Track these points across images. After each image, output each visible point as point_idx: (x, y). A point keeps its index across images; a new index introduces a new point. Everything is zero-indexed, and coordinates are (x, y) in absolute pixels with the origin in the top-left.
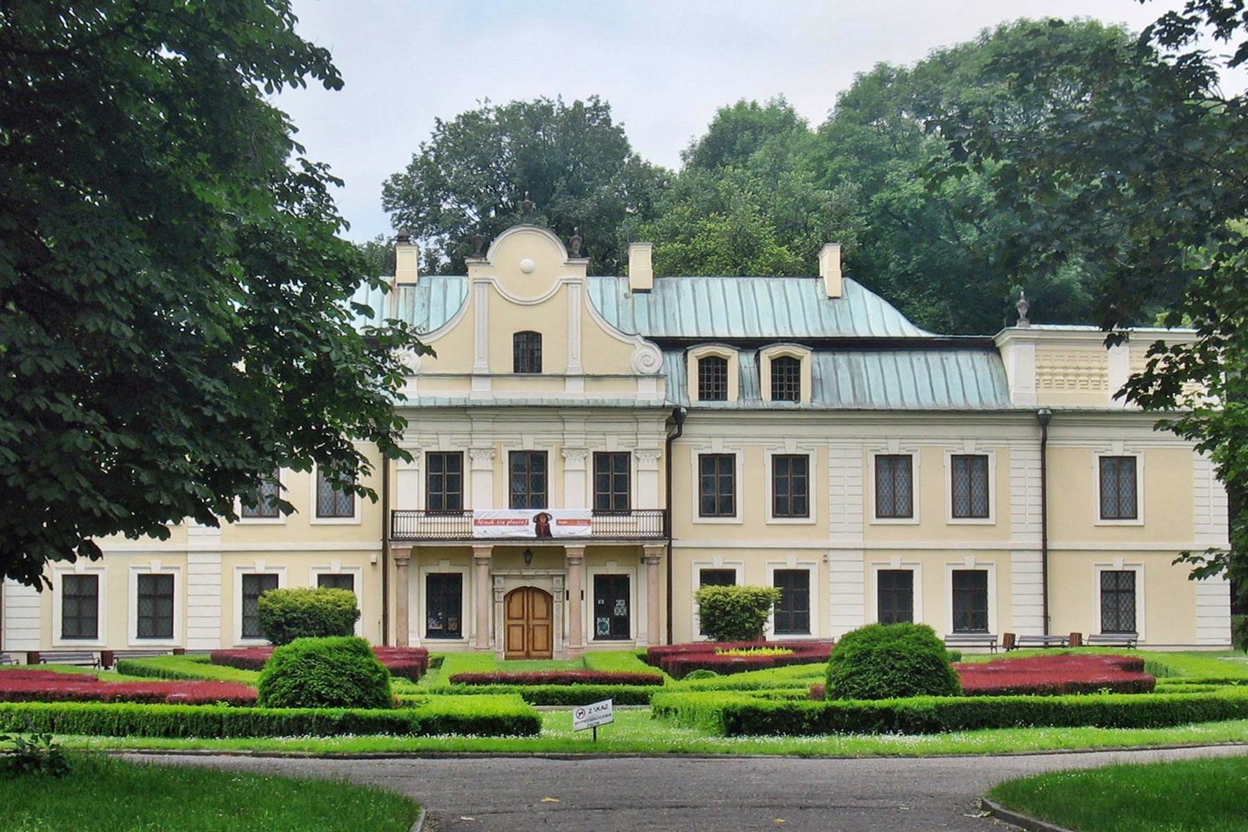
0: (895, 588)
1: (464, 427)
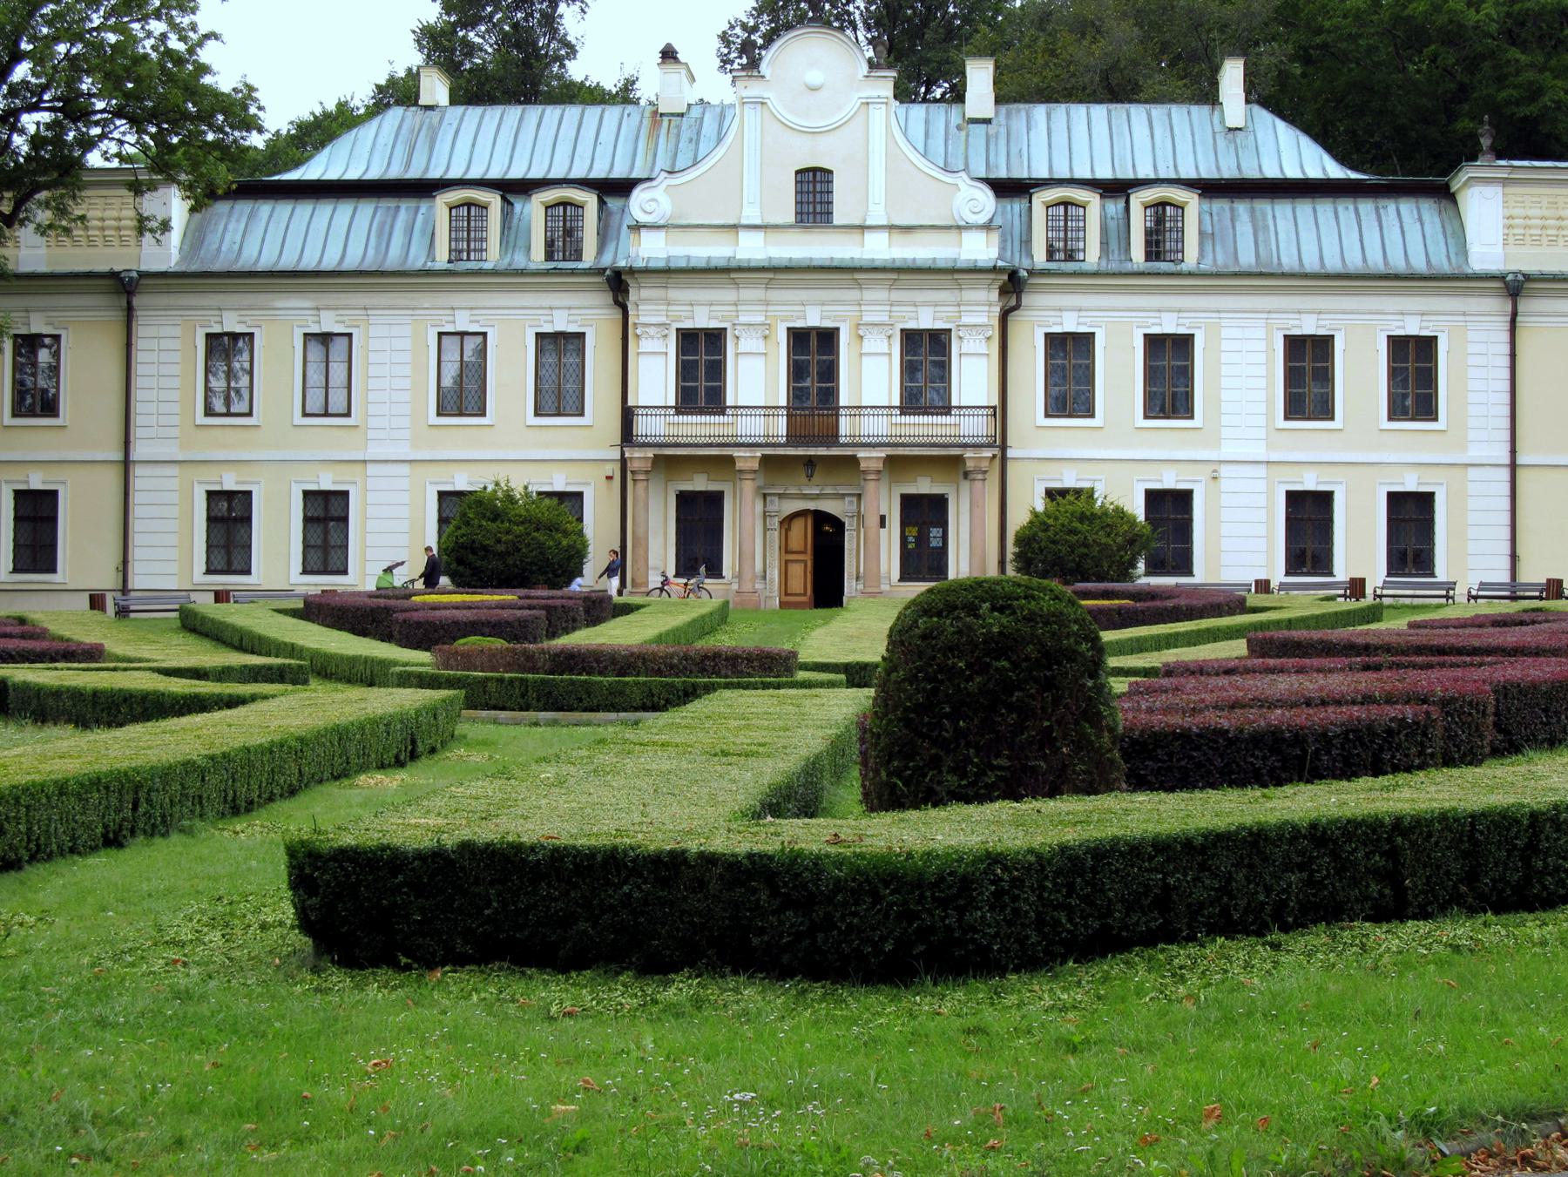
0: (1309, 518)
1: (728, 295)
